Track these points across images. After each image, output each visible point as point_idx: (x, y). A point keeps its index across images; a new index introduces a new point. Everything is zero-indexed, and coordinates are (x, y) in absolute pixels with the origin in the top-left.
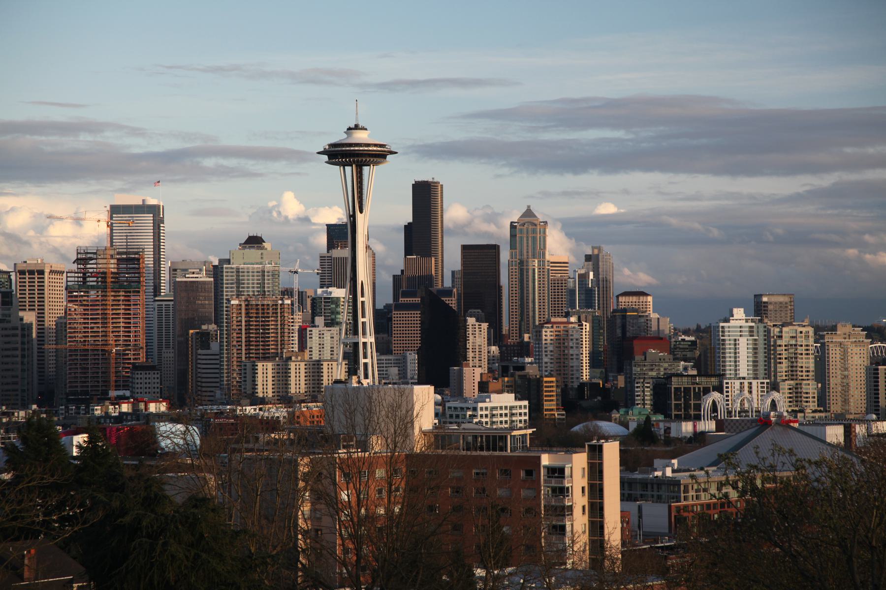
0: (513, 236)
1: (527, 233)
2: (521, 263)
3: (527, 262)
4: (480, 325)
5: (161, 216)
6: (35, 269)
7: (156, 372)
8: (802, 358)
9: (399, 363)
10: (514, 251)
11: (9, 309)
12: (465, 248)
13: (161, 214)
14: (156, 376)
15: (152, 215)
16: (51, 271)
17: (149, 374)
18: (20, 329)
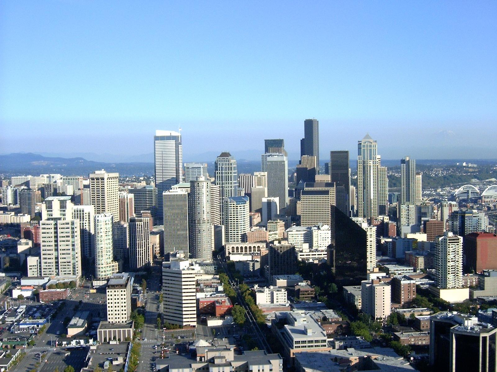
0: (360, 148)
1: (367, 147)
2: (364, 162)
3: (367, 162)
4: (371, 229)
5: (180, 141)
6: (100, 176)
7: (123, 290)
9: (308, 240)
10: (360, 156)
11: (64, 211)
12: (332, 153)
13: (180, 140)
14: (123, 293)
15: (175, 141)
16: (108, 178)
17: (118, 291)
18: (70, 224)
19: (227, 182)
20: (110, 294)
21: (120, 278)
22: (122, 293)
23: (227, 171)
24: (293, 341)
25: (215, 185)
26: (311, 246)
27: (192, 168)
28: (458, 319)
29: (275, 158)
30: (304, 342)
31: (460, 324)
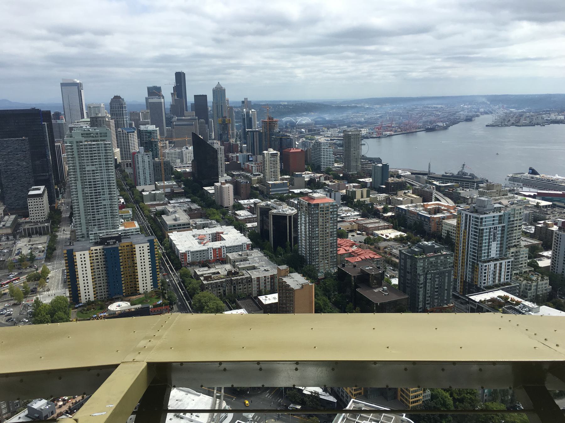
7: (41, 198)
8: (516, 230)
12: (195, 96)
14: (41, 200)
17: (36, 199)
19: (120, 117)
20: (30, 201)
21: (39, 189)
22: (39, 200)
23: (119, 110)
24: (167, 226)
25: (111, 119)
26: (182, 161)
27: (93, 107)
28: (275, 206)
29: (155, 100)
30: (174, 226)
31: (275, 209)
